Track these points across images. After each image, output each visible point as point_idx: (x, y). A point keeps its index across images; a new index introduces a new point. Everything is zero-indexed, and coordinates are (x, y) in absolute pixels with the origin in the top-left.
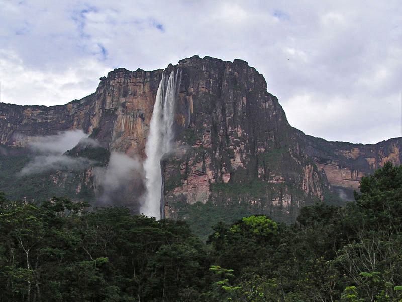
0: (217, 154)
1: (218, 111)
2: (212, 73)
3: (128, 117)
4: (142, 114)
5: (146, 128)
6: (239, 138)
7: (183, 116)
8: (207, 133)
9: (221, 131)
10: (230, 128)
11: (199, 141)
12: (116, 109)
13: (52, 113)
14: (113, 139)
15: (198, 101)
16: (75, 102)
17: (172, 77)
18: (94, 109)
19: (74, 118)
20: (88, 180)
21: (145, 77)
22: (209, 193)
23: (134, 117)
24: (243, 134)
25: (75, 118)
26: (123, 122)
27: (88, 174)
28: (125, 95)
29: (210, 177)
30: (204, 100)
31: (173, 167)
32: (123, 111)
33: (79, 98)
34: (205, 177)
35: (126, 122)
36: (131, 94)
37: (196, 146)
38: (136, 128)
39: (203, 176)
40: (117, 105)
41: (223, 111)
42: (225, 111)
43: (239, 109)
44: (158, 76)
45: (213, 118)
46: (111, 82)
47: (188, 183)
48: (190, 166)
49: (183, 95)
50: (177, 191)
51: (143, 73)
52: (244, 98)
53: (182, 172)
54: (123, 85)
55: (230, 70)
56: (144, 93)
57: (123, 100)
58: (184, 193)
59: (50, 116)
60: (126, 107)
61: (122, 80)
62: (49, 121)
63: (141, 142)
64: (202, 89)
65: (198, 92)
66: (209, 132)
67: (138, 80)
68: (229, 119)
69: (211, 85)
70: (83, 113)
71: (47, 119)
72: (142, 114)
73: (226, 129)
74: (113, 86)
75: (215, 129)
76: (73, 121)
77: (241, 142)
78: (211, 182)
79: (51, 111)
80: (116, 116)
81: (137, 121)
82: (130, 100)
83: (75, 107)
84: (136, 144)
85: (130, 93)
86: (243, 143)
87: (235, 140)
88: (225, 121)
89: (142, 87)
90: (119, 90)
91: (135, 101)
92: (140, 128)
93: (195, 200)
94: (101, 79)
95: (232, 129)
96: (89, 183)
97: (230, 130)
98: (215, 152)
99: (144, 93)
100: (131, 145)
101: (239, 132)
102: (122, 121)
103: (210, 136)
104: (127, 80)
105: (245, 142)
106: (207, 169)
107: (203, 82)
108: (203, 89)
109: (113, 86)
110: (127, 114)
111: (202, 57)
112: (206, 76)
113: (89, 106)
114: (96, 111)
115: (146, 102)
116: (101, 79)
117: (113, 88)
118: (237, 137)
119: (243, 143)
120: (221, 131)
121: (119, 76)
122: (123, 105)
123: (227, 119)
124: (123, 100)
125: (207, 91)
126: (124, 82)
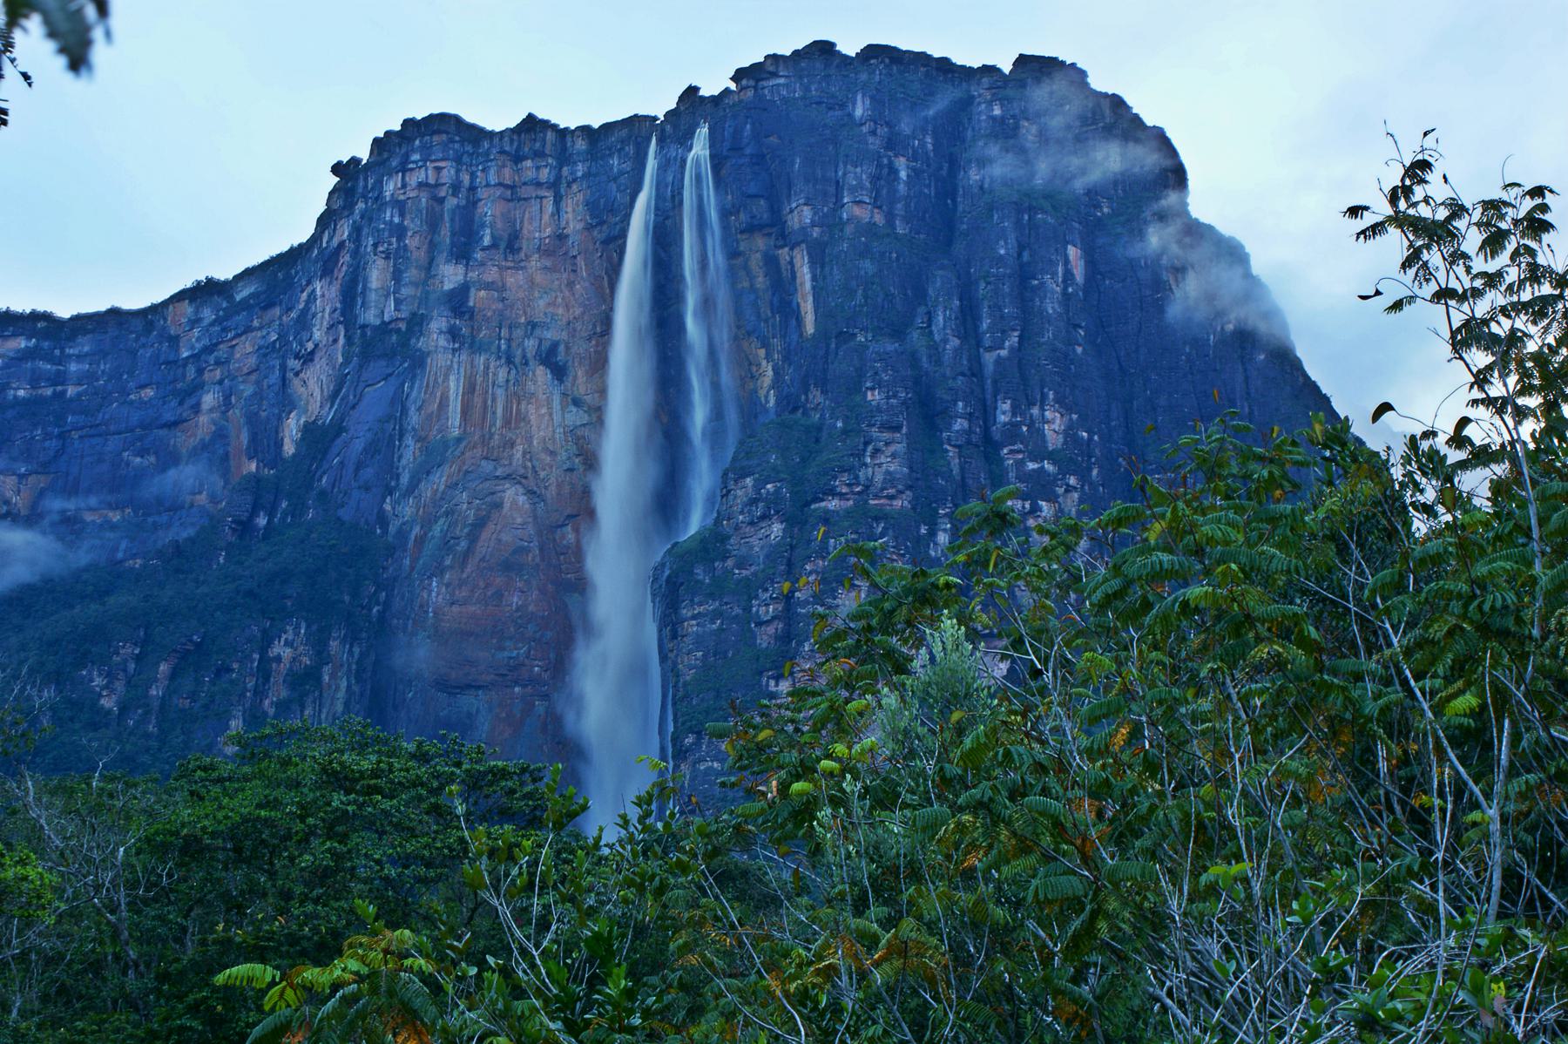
0: (943, 538)
1: (940, 318)
2: (905, 127)
3: (481, 360)
4: (554, 346)
5: (575, 417)
6: (1051, 456)
7: (762, 352)
8: (886, 435)
9: (960, 424)
10: (1006, 406)
11: (845, 477)
12: (417, 323)
13: (86, 349)
14: (405, 479)
15: (837, 275)
16: (206, 291)
17: (700, 148)
18: (304, 322)
19: (200, 371)
20: (278, 691)
21: (564, 157)
23: (509, 361)
24: (1069, 433)
25: (206, 376)
26: (455, 387)
27: (278, 659)
28: (462, 254)
30: (868, 266)
31: (717, 614)
32: (453, 334)
33: (225, 273)
35: (470, 389)
36: (494, 245)
37: (833, 504)
38: (523, 418)
40: (424, 300)
41: (968, 317)
42: (977, 319)
43: (1051, 307)
44: (630, 149)
45: (914, 358)
46: (390, 187)
48: (806, 602)
49: (760, 243)
51: (550, 135)
52: (1072, 252)
53: (765, 638)
54: (451, 202)
55: (997, 111)
56: (561, 237)
57: (451, 275)
59: (73, 367)
60: (472, 312)
61: (448, 175)
62: (71, 391)
63: (553, 488)
64: (857, 211)
65: (831, 222)
66: (897, 428)
67: (530, 174)
68: (999, 361)
69: (902, 188)
70: (246, 350)
71: (59, 379)
73: (985, 413)
74: (401, 206)
75: (927, 413)
76: (197, 388)
77: (1064, 472)
79: (80, 339)
80: (419, 361)
81: (530, 387)
82: (491, 274)
83: (208, 315)
84: (522, 499)
85: (487, 241)
86: (1072, 481)
87: (1032, 466)
88: (976, 371)
89: (549, 207)
90: (433, 224)
91: (514, 280)
92: (546, 416)
94: (337, 169)
95: (1015, 410)
96: (283, 707)
97: (1002, 418)
98: (932, 534)
99: (561, 237)
100: (498, 506)
101: (1054, 424)
102: (452, 384)
103: (899, 447)
104: (473, 176)
105: (1084, 476)
107: (857, 175)
108: (858, 212)
109: (401, 206)
110: (475, 347)
111: (849, 46)
112: (874, 143)
113: (277, 311)
114: (317, 335)
115: (571, 285)
116: (337, 169)
117: (402, 215)
118: (1040, 454)
119: (1072, 481)
120: (960, 424)
121: (427, 152)
122: (457, 301)
123: (989, 358)
124: (451, 275)
125: (879, 218)
126: (456, 188)
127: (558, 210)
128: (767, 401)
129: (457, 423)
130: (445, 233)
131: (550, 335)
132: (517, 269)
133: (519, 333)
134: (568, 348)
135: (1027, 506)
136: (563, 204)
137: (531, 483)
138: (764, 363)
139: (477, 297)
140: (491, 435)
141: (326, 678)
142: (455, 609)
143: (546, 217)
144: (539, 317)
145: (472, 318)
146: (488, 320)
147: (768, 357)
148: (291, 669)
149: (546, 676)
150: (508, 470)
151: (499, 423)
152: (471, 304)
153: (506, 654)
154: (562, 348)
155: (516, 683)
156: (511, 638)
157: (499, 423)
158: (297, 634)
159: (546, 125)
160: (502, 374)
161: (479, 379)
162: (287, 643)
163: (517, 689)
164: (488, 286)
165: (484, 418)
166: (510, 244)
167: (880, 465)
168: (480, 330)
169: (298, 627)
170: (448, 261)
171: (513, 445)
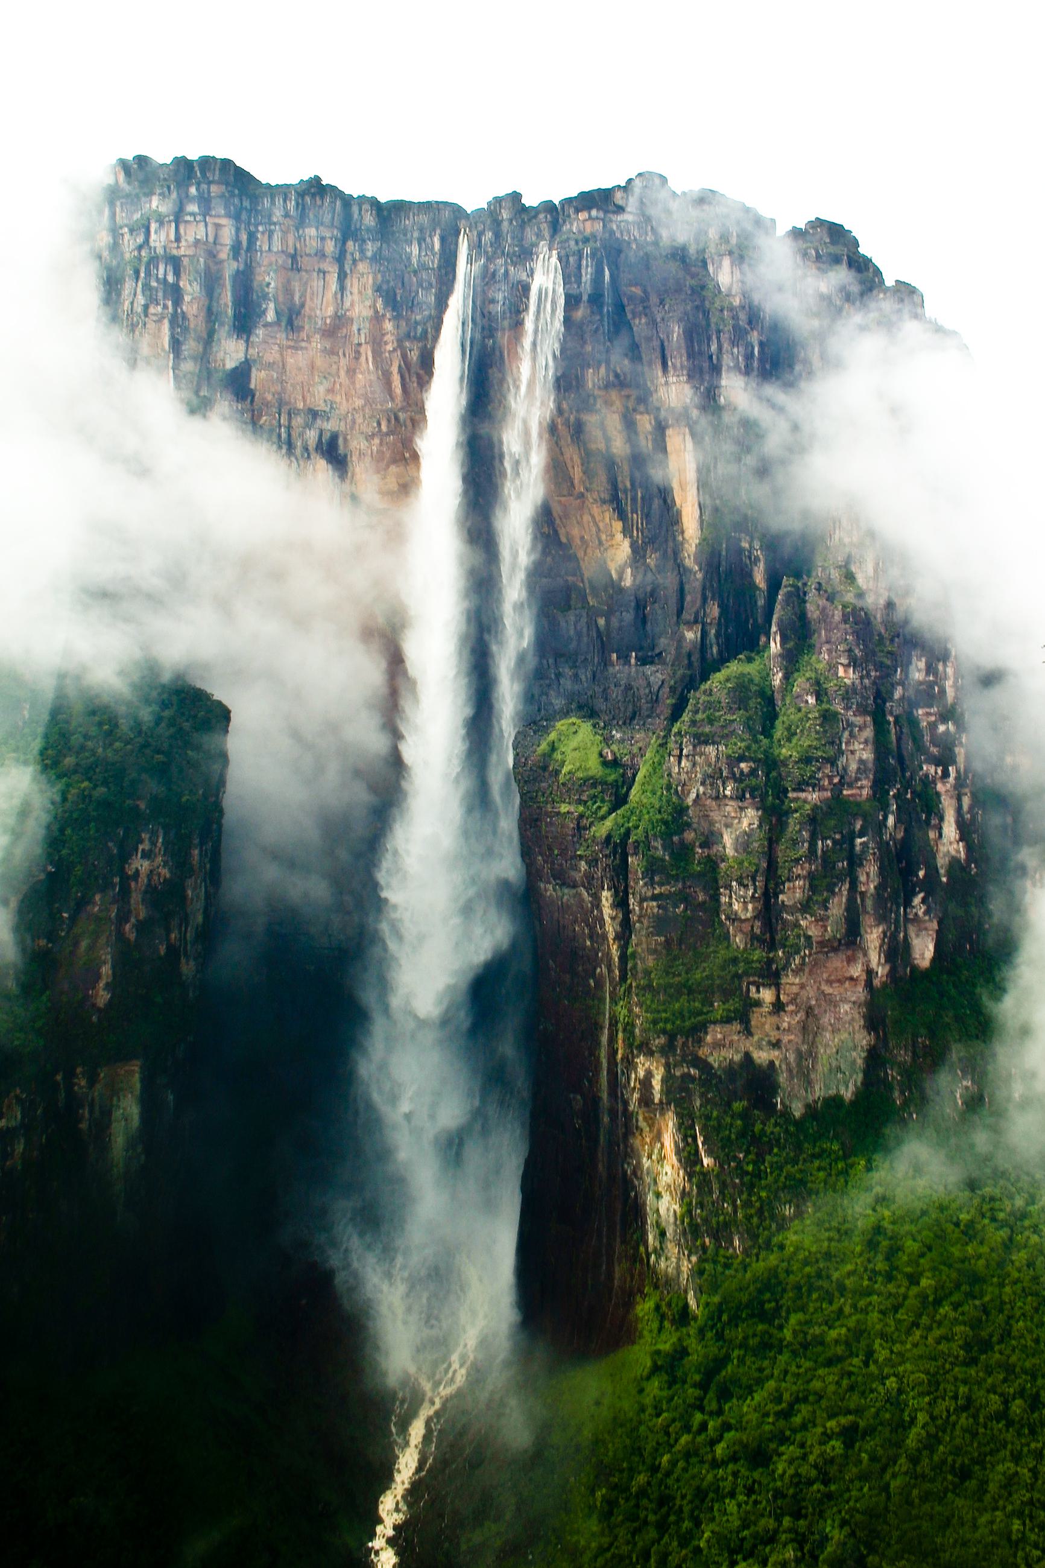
0: (891, 820)
4: (334, 437)
7: (618, 525)
22: (864, 1039)
29: (874, 957)
34: (851, 960)
36: (278, 323)
39: (842, 956)
47: (778, 1007)
48: (792, 910)
50: (718, 1045)
58: (762, 1056)
72: (334, 437)
74: (176, 263)
78: (876, 982)
82: (272, 355)
85: (270, 316)
89: (334, 286)
91: (296, 361)
93: (809, 1083)
98: (885, 818)
106: (867, 920)
115: (351, 372)
117: (177, 273)
127: (342, 288)
128: (621, 578)
130: (227, 298)
131: (330, 426)
132: (296, 348)
133: (298, 421)
134: (345, 440)
135: (939, 772)
136: (348, 282)
138: (619, 536)
139: (258, 378)
141: (189, 893)
143: (329, 295)
144: (321, 406)
145: (252, 401)
146: (267, 404)
147: (626, 531)
148: (149, 885)
152: (252, 386)
154: (341, 441)
158: (153, 843)
159: (333, 191)
162: (146, 855)
164: (270, 366)
166: (291, 319)
167: (853, 752)
168: (260, 416)
169: (154, 834)
170: (229, 336)
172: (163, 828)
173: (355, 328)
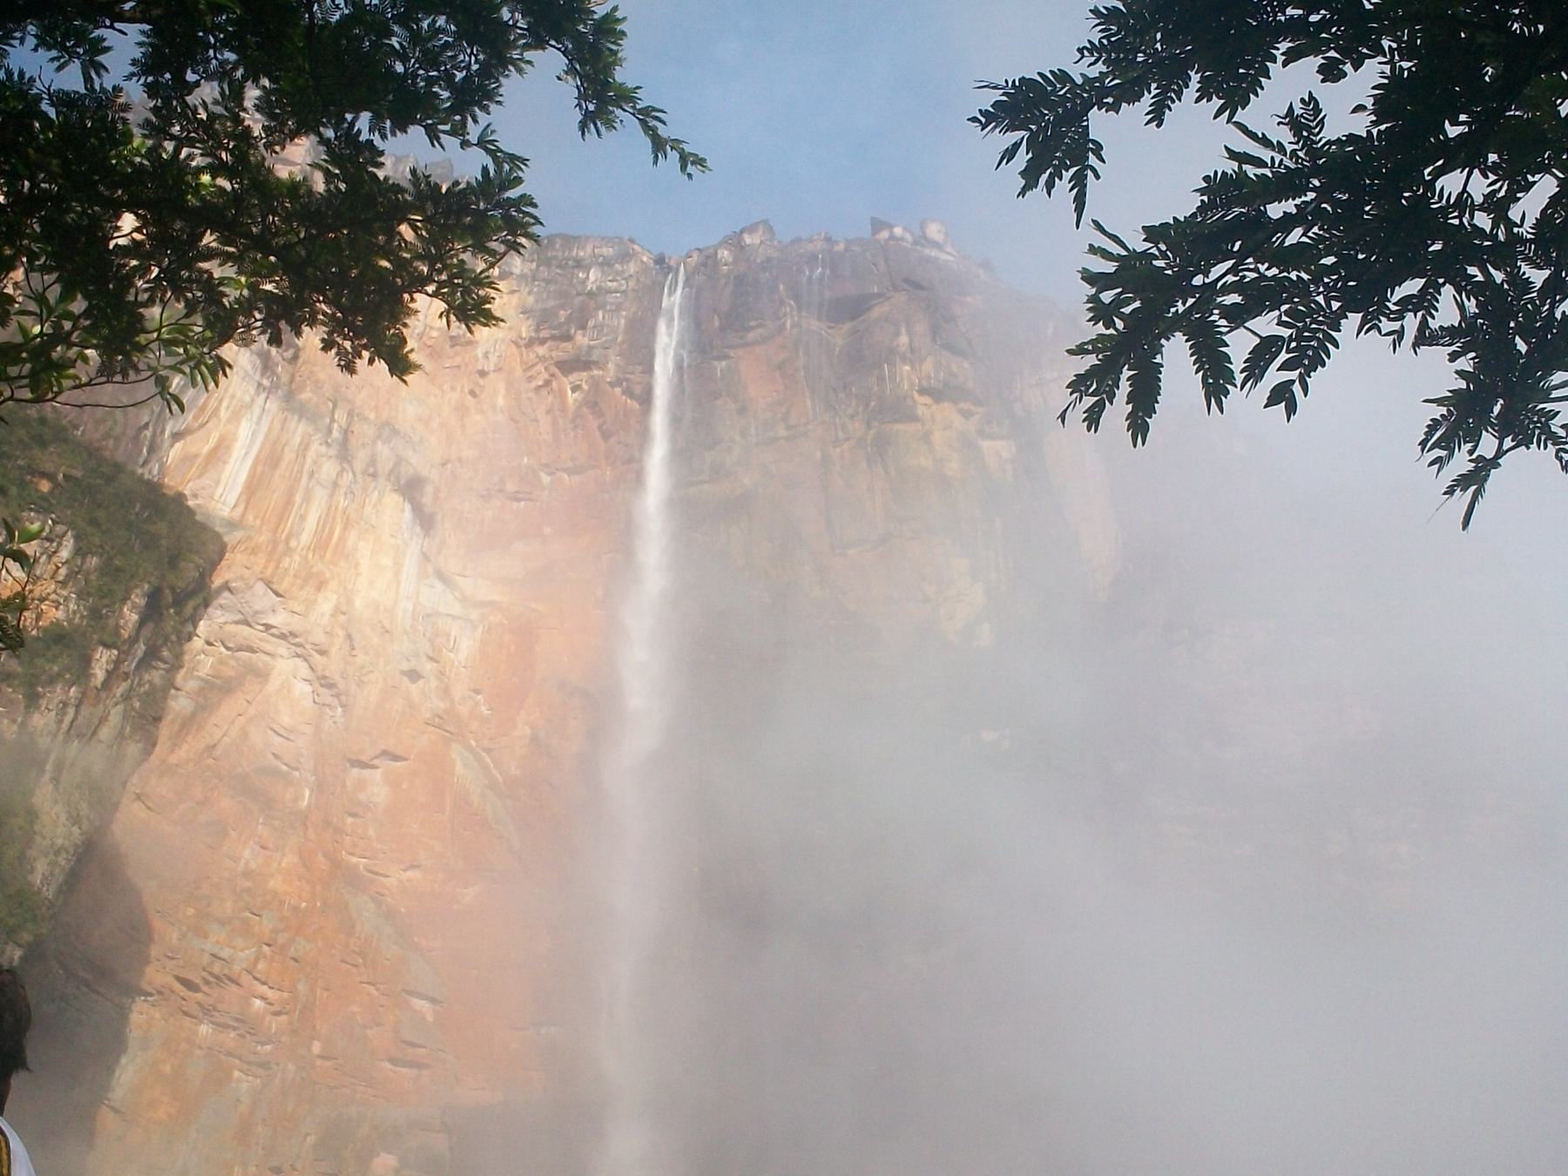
5: (435, 597)
23: (344, 455)
35: (269, 459)
84: (302, 689)
129: (232, 498)
137: (332, 666)
140: (289, 551)
142: (137, 805)
149: (275, 1024)
150: (296, 624)
151: (306, 538)
153: (208, 946)
155: (207, 1011)
156: (222, 923)
157: (306, 538)
160: (329, 469)
161: (289, 455)
163: (205, 1029)
165: (281, 518)
168: (302, 388)
171: (321, 585)
172: (77, 538)
173: (479, 352)
